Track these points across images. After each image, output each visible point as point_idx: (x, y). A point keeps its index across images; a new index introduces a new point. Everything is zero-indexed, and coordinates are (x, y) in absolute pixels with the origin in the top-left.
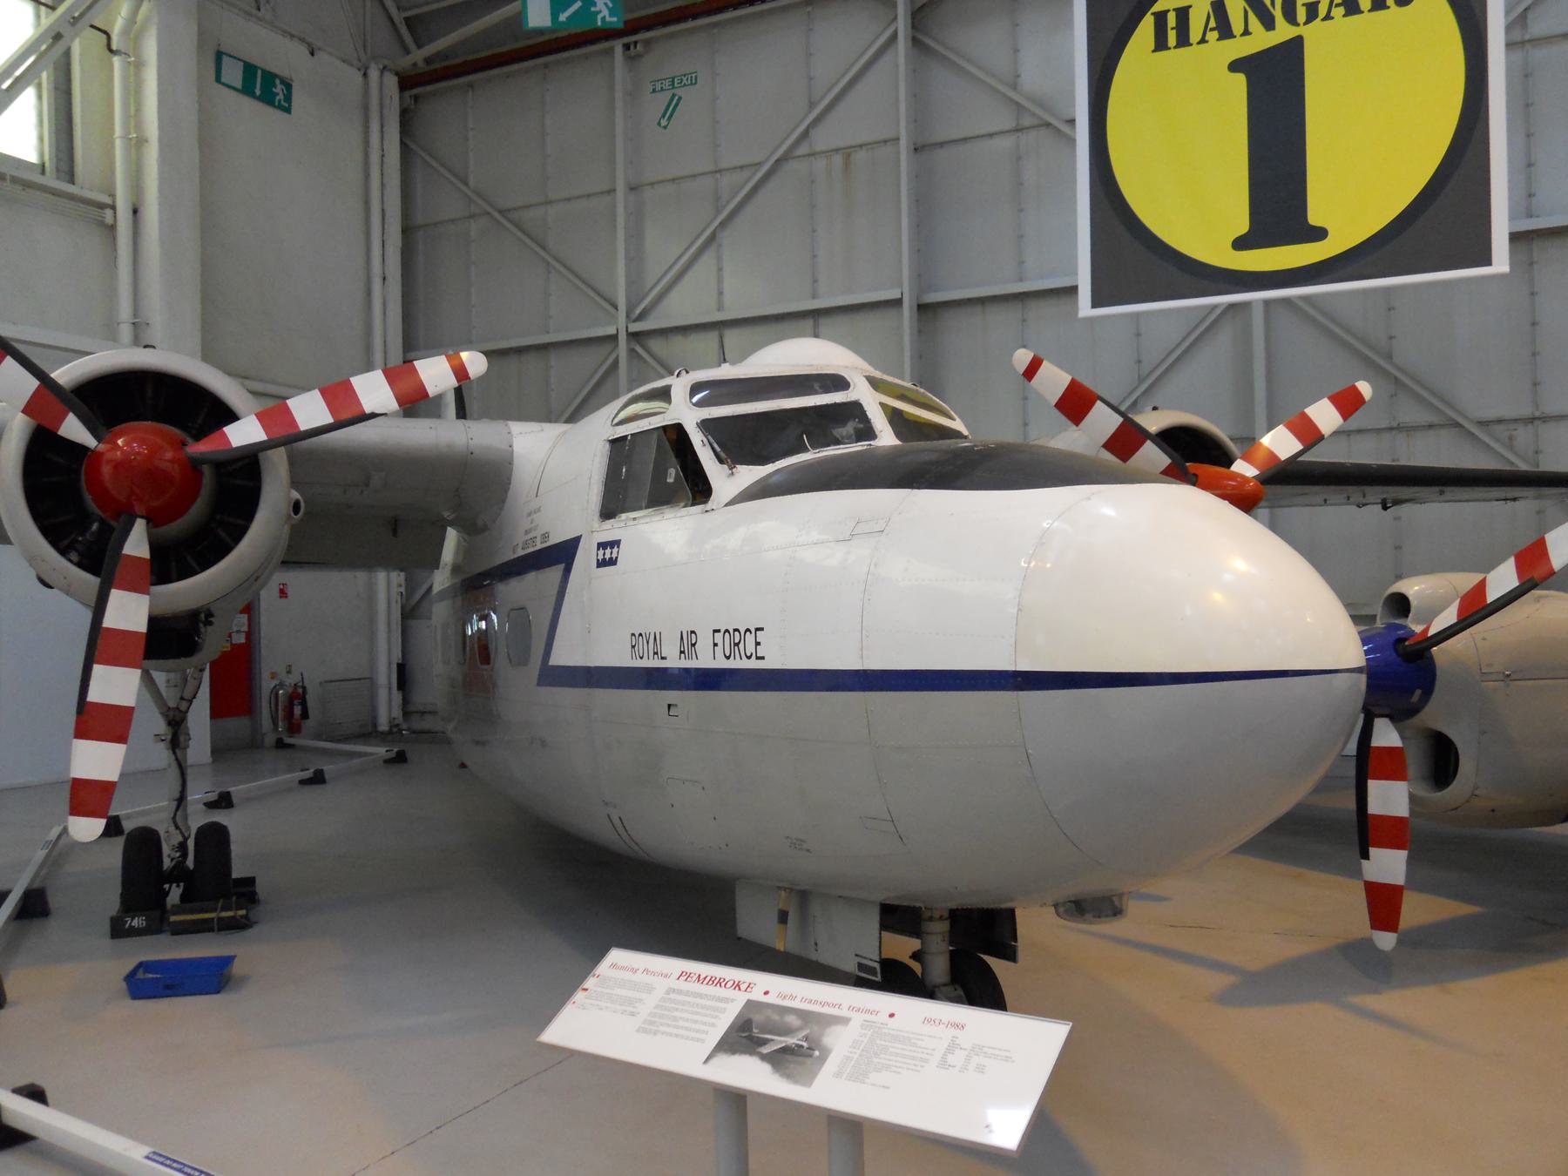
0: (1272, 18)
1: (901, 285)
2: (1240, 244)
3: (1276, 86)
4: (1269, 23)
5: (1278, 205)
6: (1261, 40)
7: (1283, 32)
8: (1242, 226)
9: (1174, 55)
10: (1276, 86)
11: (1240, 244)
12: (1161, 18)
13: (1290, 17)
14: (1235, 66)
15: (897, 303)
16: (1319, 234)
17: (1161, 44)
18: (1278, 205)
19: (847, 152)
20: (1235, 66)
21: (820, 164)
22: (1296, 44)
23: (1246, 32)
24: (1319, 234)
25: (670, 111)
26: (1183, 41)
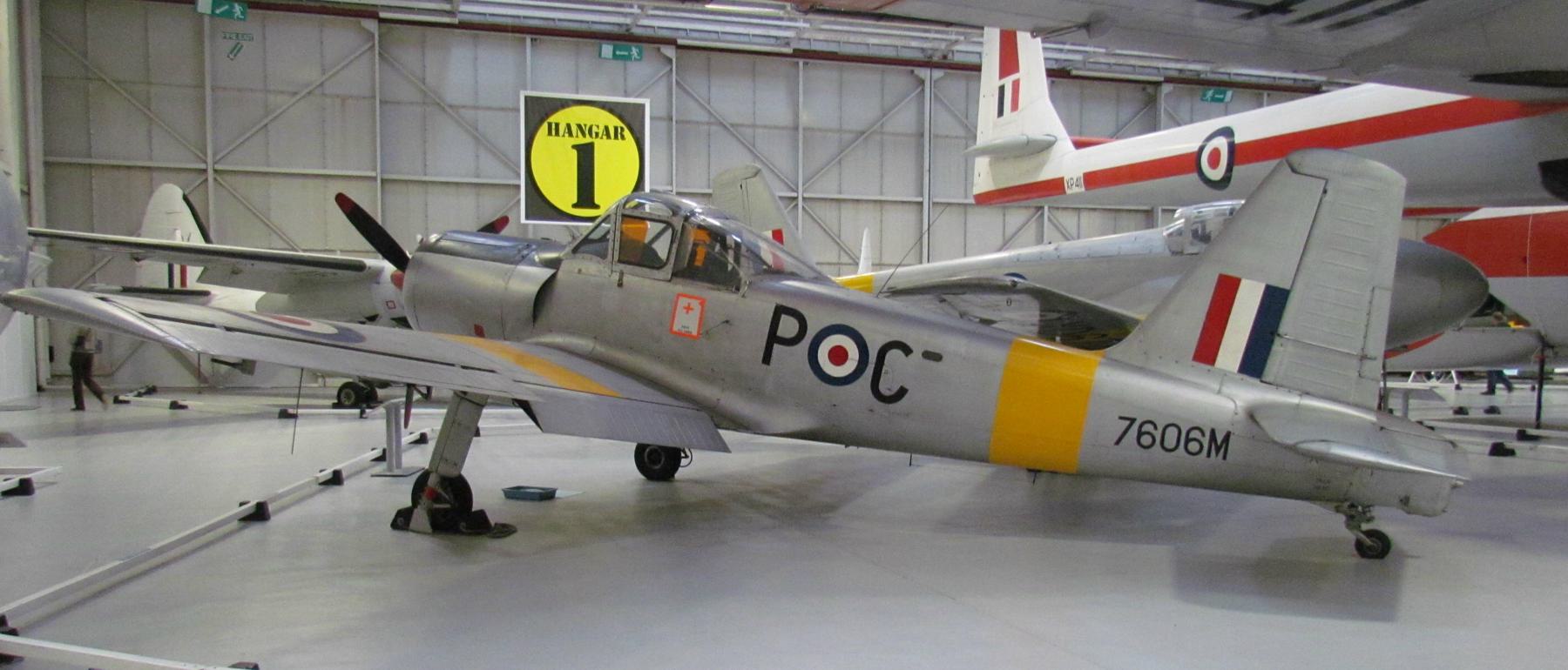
1: (375, 169)
2: (575, 206)
3: (585, 155)
5: (586, 195)
6: (582, 140)
7: (588, 140)
9: (553, 138)
10: (585, 155)
11: (575, 206)
12: (550, 125)
14: (574, 147)
15: (375, 179)
16: (597, 207)
17: (550, 133)
18: (586, 195)
19: (344, 99)
20: (574, 147)
21: (328, 101)
24: (597, 207)
25: (236, 50)
26: (557, 134)
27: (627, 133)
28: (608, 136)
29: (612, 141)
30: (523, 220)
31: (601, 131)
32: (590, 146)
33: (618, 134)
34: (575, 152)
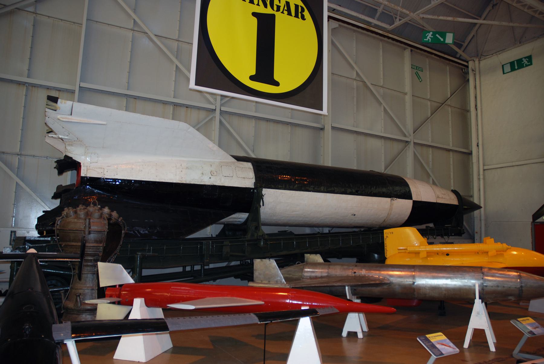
0: (267, 4)
2: (252, 78)
4: (266, 6)
5: (265, 70)
7: (269, 11)
8: (253, 73)
11: (252, 78)
13: (272, 7)
14: (254, 14)
16: (277, 84)
18: (265, 70)
20: (254, 14)
22: (273, 16)
23: (258, 5)
24: (277, 84)
27: (306, 13)
28: (290, 14)
29: (292, 19)
30: (192, 84)
31: (282, 4)
32: (272, 17)
33: (298, 14)
34: (255, 20)
